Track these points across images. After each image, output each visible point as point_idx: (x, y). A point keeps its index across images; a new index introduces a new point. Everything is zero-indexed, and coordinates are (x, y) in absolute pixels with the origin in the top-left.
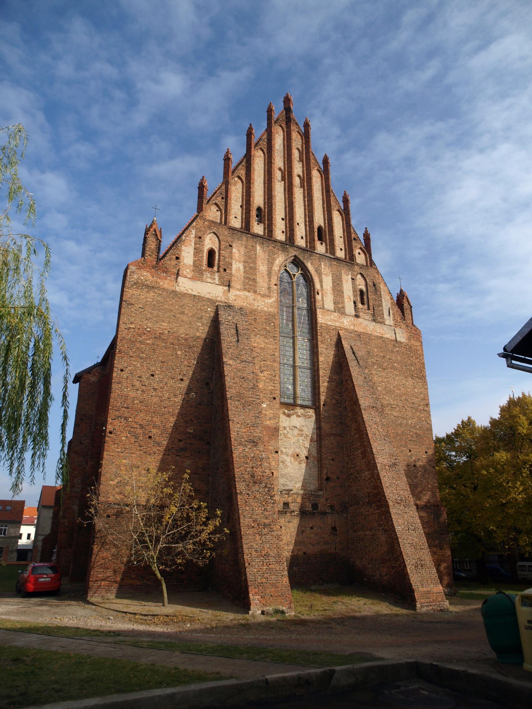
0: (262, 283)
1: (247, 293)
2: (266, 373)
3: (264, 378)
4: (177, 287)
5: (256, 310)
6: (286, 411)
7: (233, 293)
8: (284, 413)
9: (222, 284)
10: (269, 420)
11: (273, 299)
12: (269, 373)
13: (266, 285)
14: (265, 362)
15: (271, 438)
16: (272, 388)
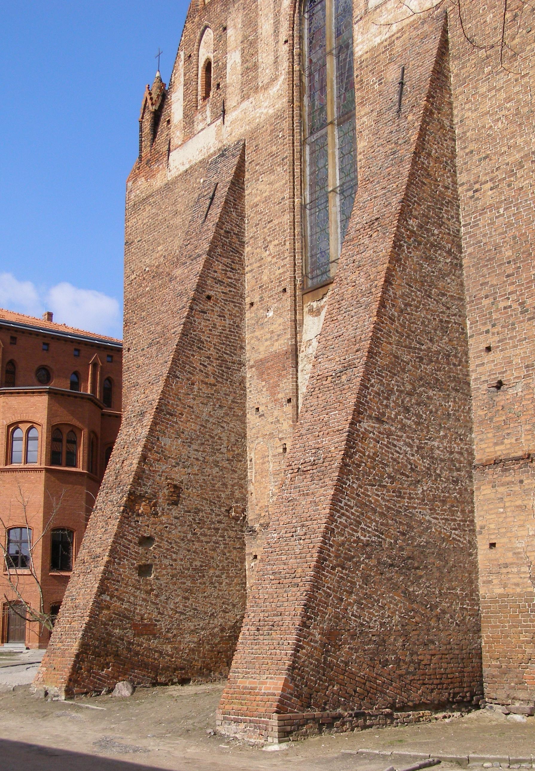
0: (265, 58)
1: (246, 104)
2: (271, 247)
3: (269, 259)
4: (169, 174)
5: (257, 128)
6: (315, 304)
7: (229, 118)
8: (311, 311)
9: (215, 118)
10: (277, 340)
11: (282, 78)
12: (276, 242)
13: (271, 58)
14: (270, 225)
15: (280, 375)
16: (281, 271)
